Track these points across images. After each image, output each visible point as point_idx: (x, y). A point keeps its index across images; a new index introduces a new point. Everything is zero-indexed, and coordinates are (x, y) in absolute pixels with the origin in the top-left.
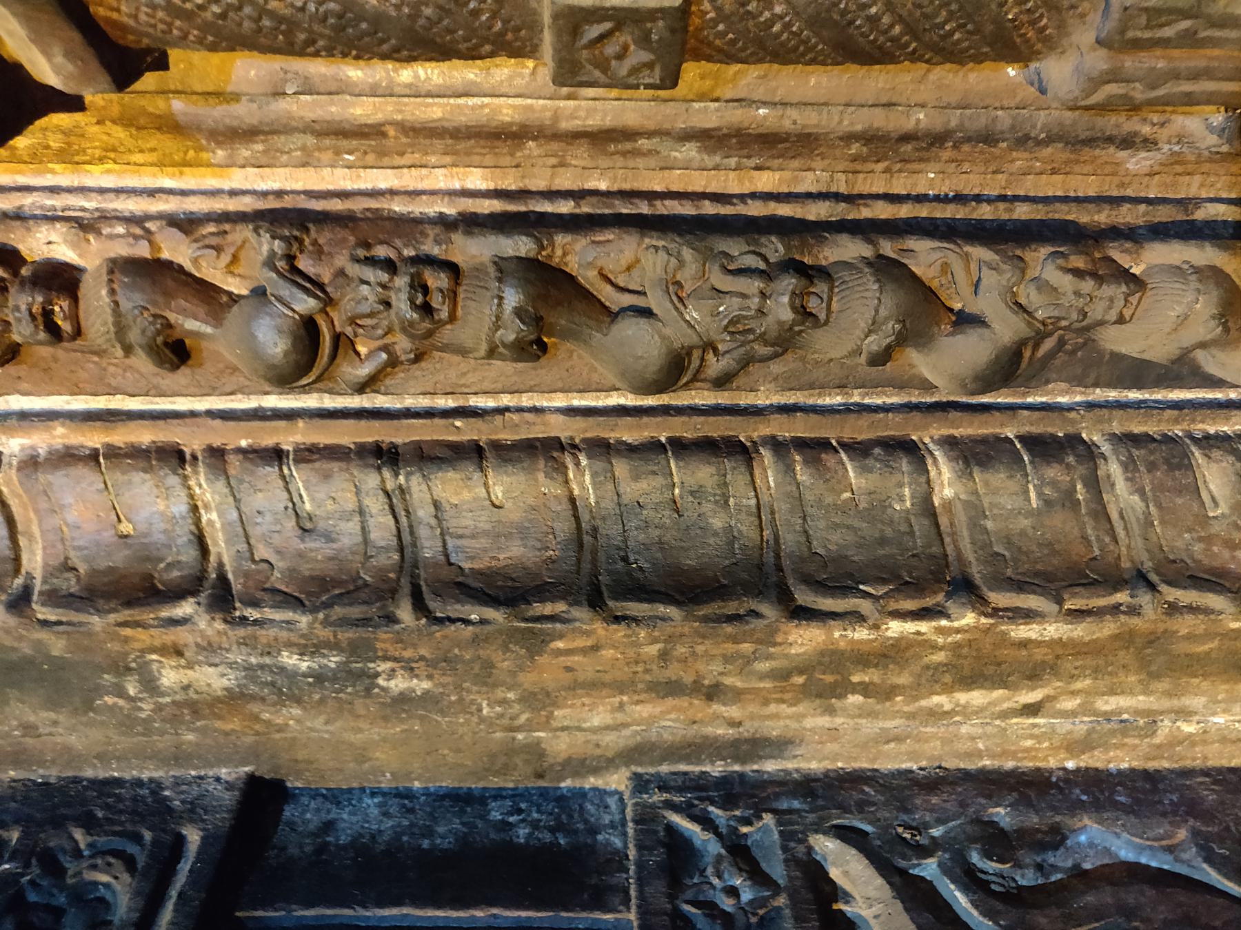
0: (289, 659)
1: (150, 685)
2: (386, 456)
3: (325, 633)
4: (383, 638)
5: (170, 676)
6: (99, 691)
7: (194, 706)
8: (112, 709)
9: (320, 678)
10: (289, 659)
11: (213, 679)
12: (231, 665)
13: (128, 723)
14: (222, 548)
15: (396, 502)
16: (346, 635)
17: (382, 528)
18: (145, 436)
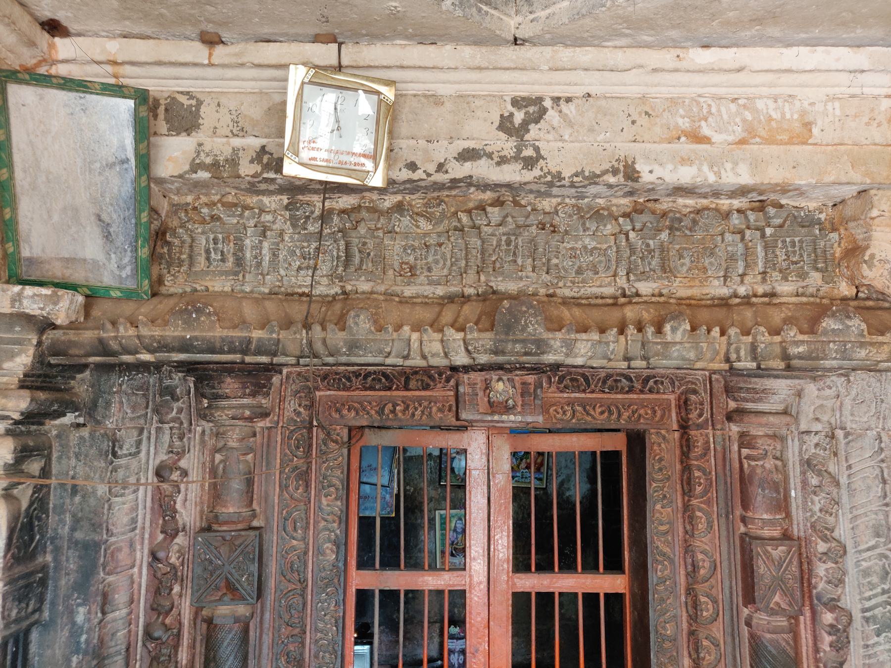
0: (84, 638)
1: (79, 605)
2: (128, 649)
3: (92, 645)
4: (89, 658)
5: (82, 610)
6: (79, 594)
7: (71, 613)
8: (73, 595)
9: (78, 643)
10: (84, 638)
11: (80, 618)
12: (84, 624)
13: (68, 597)
14: (110, 616)
15: (118, 653)
16: (91, 651)
17: (112, 650)
18: (135, 597)
